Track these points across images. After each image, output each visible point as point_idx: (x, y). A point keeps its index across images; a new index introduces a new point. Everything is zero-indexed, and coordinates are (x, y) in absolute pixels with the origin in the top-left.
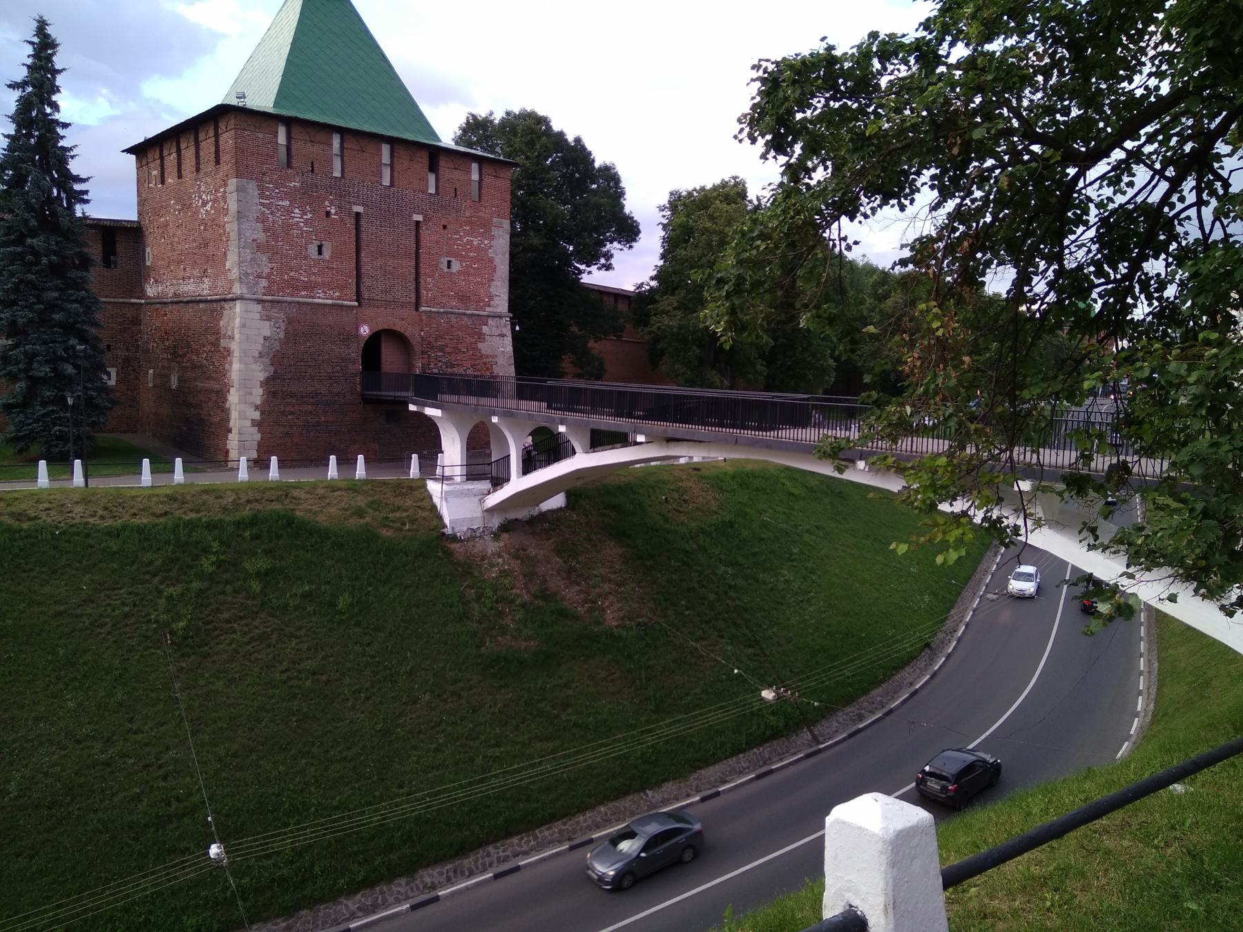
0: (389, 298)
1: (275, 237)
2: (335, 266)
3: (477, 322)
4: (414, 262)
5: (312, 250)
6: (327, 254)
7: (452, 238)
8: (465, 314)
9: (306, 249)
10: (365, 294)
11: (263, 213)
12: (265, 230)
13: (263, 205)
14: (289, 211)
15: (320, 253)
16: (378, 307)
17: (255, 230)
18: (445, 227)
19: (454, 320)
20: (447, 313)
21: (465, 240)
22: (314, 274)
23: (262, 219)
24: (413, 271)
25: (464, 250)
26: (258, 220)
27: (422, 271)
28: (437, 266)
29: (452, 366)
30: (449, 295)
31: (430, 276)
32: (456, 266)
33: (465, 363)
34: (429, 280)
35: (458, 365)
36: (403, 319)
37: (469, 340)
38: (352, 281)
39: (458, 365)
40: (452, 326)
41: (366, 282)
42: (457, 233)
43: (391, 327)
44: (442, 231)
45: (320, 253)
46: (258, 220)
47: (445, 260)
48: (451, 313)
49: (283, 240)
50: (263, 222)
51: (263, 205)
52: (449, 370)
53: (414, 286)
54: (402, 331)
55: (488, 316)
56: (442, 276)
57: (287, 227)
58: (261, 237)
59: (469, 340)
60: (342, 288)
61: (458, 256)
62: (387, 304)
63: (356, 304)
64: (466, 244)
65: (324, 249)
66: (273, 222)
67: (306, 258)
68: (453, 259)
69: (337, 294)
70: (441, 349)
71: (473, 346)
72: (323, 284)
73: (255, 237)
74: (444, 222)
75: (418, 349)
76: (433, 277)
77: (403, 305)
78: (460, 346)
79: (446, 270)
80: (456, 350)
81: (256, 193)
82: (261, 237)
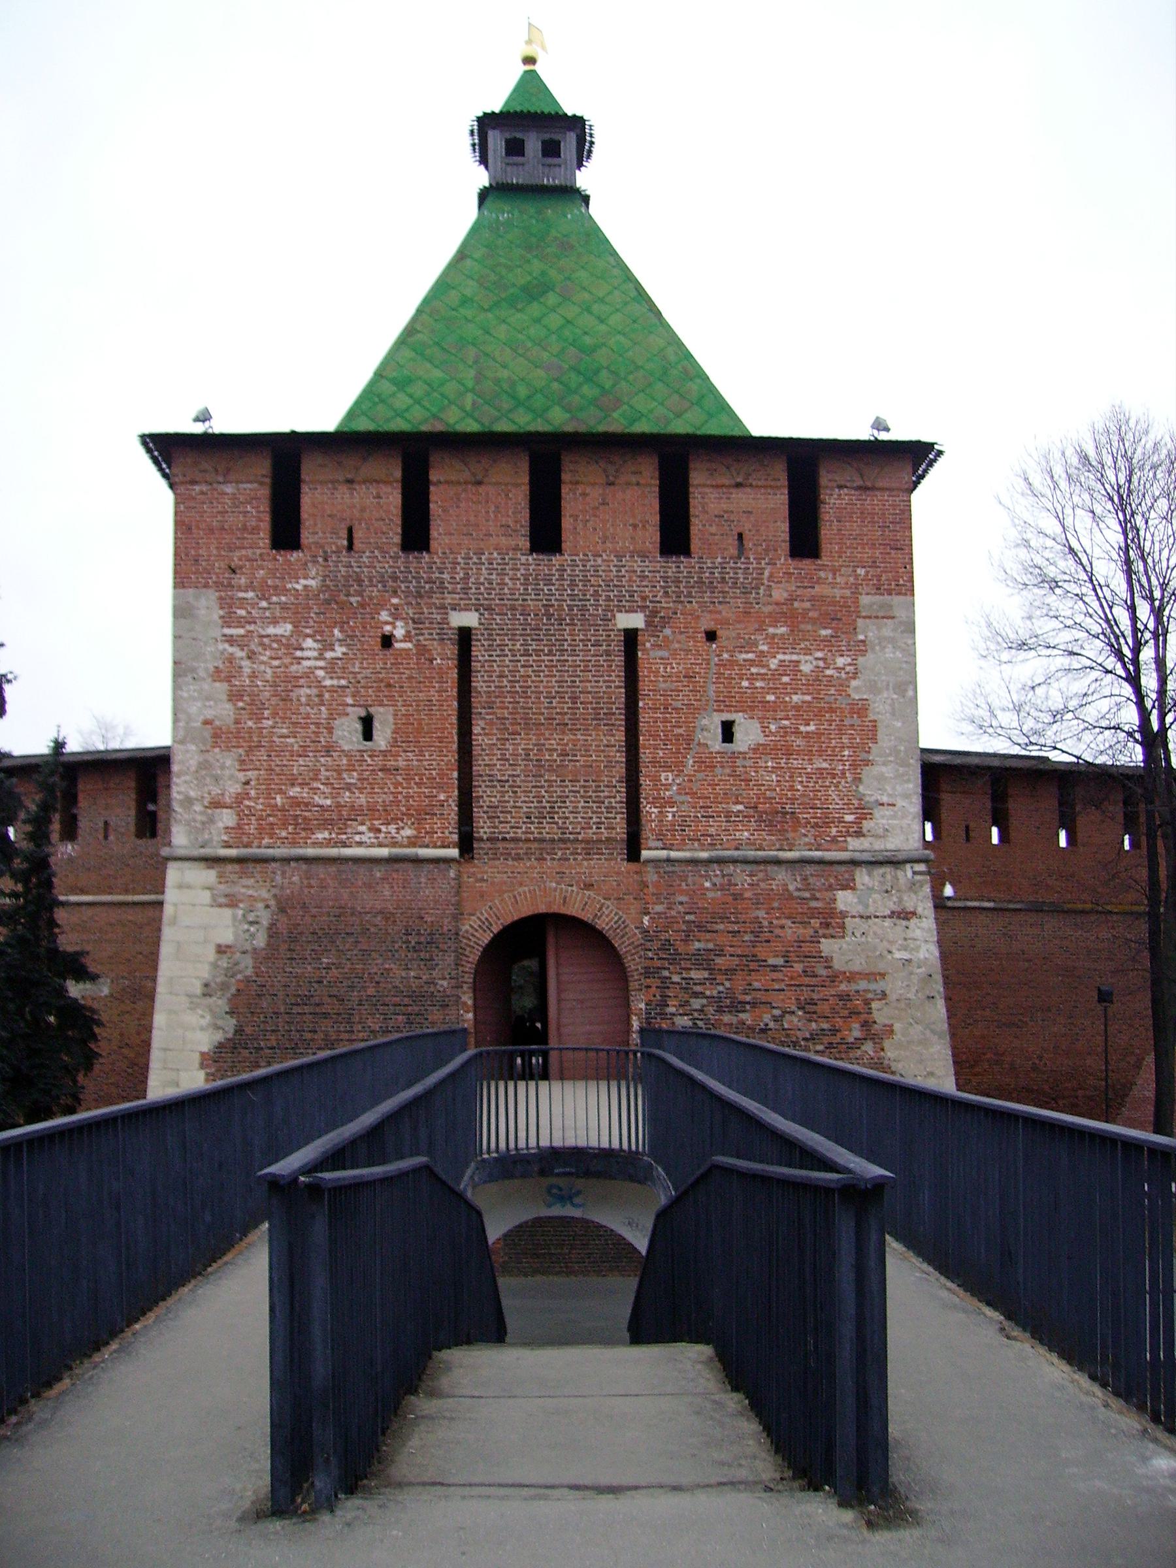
0: (548, 830)
1: (256, 710)
2: (401, 763)
3: (814, 881)
4: (620, 736)
5: (347, 732)
6: (382, 737)
7: (732, 663)
8: (778, 862)
9: (330, 730)
10: (483, 828)
11: (231, 659)
12: (235, 696)
13: (230, 640)
14: (290, 647)
15: (368, 735)
16: (518, 858)
17: (208, 699)
18: (711, 636)
19: (742, 878)
20: (720, 861)
21: (773, 663)
22: (349, 787)
23: (226, 673)
24: (621, 758)
25: (770, 690)
26: (217, 675)
27: (645, 755)
28: (689, 740)
29: (737, 1006)
30: (728, 814)
31: (667, 767)
32: (748, 733)
33: (777, 999)
34: (666, 777)
35: (754, 1004)
36: (589, 886)
37: (791, 931)
38: (449, 798)
39: (754, 1004)
40: (737, 897)
41: (485, 795)
42: (751, 645)
43: (555, 909)
44: (703, 645)
45: (368, 735)
46: (217, 675)
47: (713, 723)
48: (735, 861)
49: (275, 714)
50: (228, 679)
51: (230, 640)
52: (726, 1018)
53: (622, 796)
54: (587, 917)
55: (854, 863)
56: (706, 763)
57: (285, 684)
58: (224, 712)
59: (791, 931)
60: (420, 815)
61: (754, 706)
62: (544, 847)
63: (454, 852)
64: (776, 675)
65: (376, 724)
66: (253, 676)
67: (328, 750)
68: (738, 717)
69: (408, 832)
70: (703, 960)
71: (806, 948)
72: (372, 809)
73: (209, 714)
74: (706, 624)
75: (634, 964)
76: (677, 767)
77: (591, 847)
78: (761, 951)
79: (717, 745)
80: (752, 963)
81: (217, 614)
82: (224, 712)
